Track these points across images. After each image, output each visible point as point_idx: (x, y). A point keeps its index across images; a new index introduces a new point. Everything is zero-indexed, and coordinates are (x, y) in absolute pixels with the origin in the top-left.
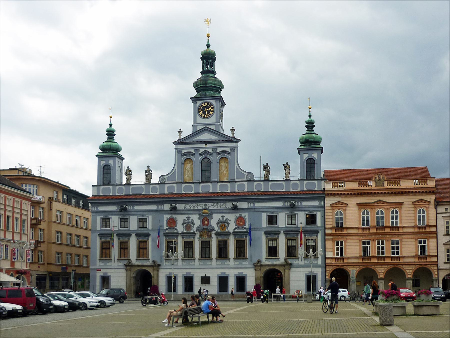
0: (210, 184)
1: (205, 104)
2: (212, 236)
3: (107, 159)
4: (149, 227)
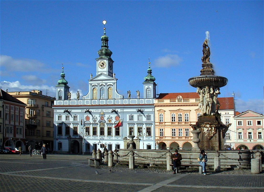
0: (104, 100)
2: (104, 125)
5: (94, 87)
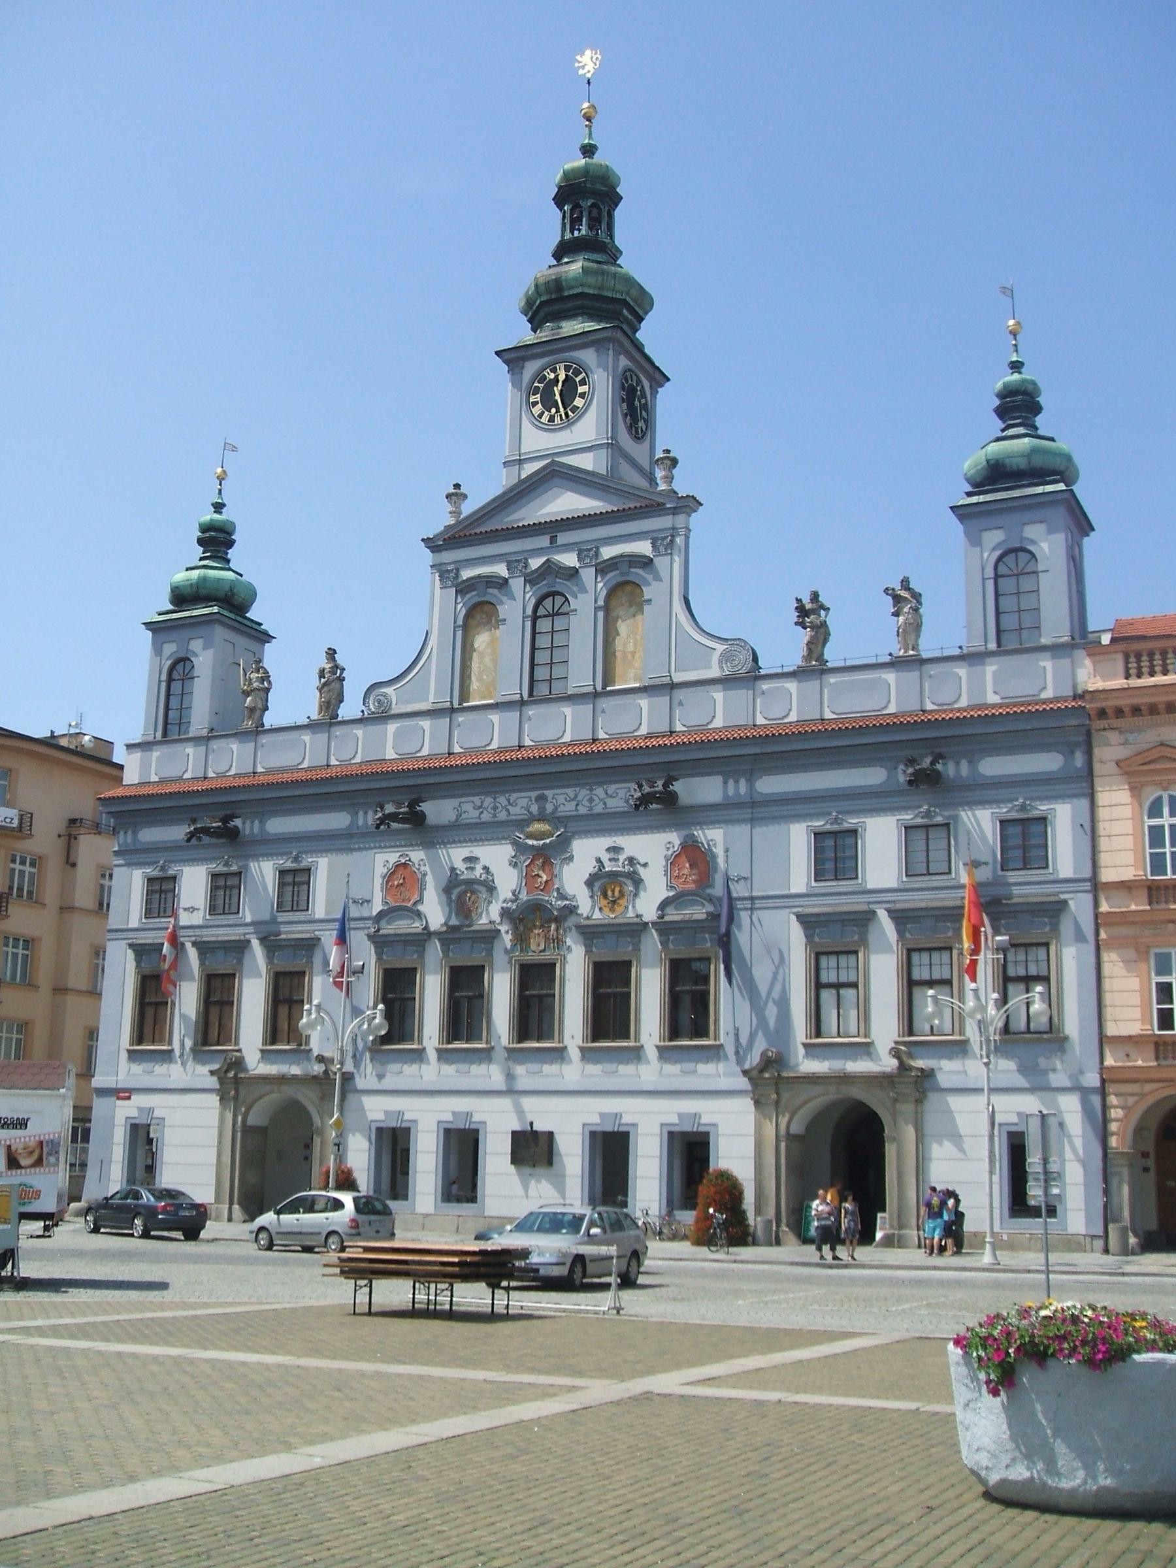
1: (554, 370)
2: (559, 942)
3: (184, 634)
4: (316, 911)
5: (472, 597)
